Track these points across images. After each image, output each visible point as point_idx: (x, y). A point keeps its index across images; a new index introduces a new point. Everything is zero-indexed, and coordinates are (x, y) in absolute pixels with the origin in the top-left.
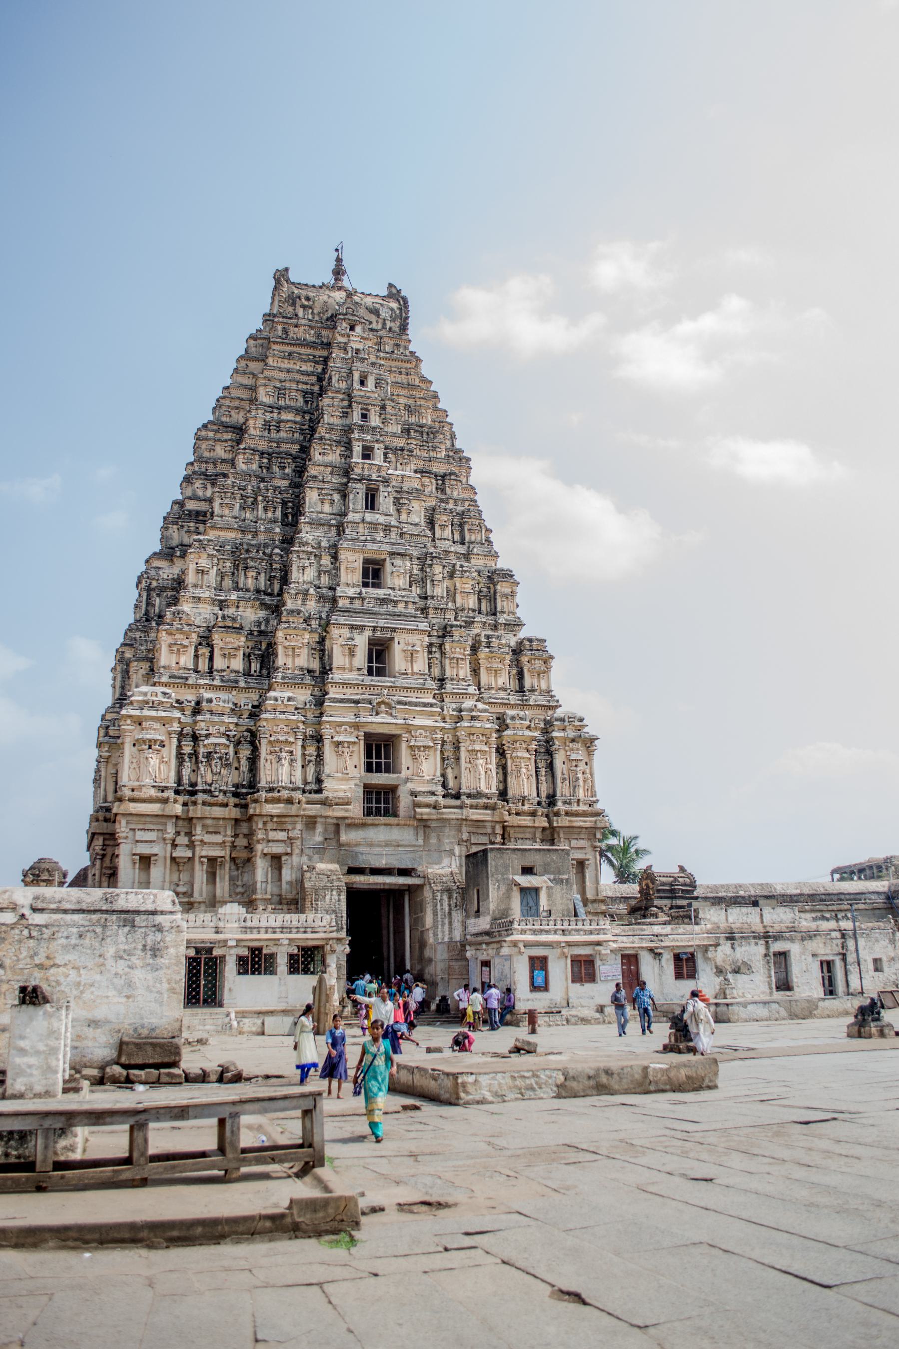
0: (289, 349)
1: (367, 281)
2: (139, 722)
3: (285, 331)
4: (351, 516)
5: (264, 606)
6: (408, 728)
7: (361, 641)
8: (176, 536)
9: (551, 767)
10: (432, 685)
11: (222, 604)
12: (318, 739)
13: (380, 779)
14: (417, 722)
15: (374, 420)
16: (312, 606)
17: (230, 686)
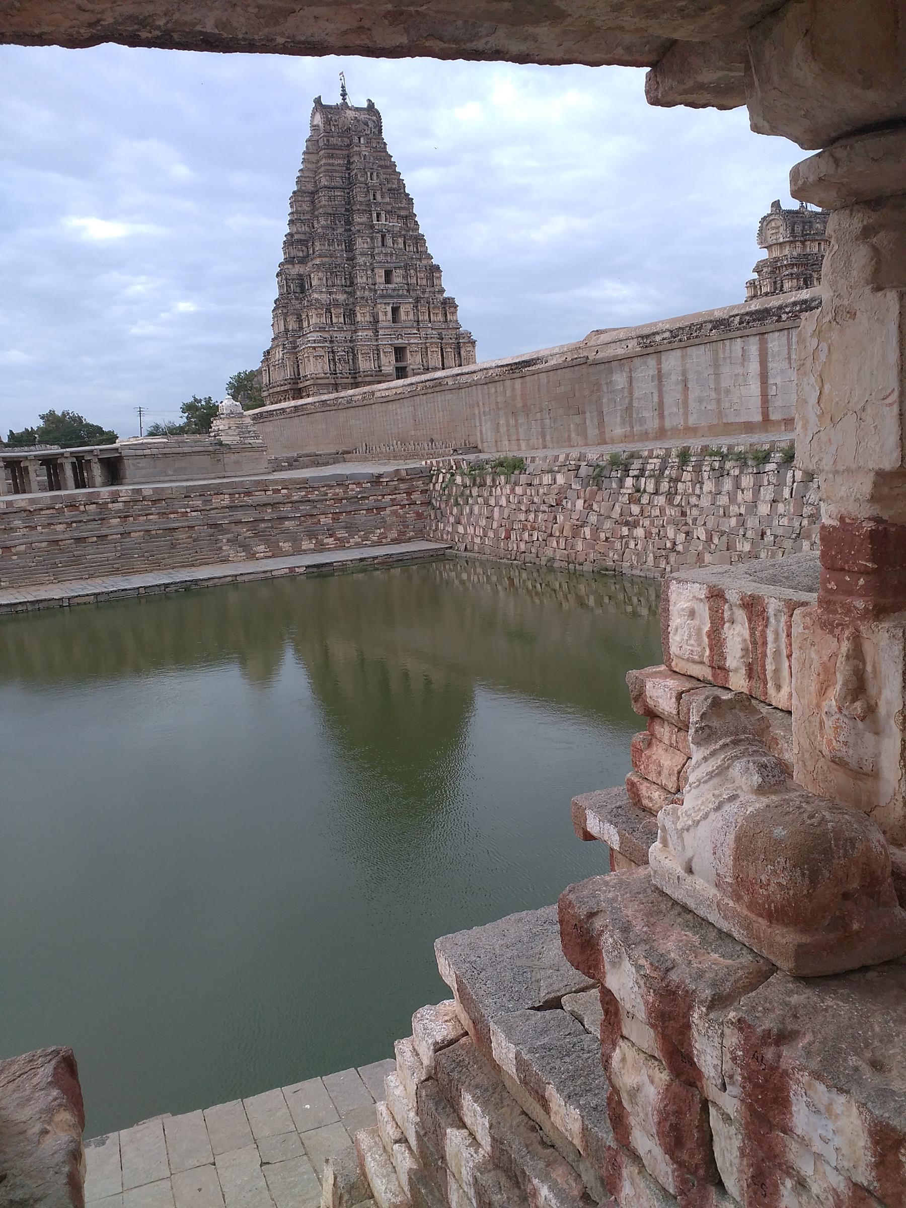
0: (331, 151)
1: (357, 100)
2: (314, 348)
3: (328, 141)
4: (376, 251)
5: (346, 292)
6: (409, 344)
7: (389, 309)
8: (294, 252)
9: (459, 353)
10: (415, 324)
11: (330, 293)
12: (378, 350)
13: (400, 364)
14: (412, 341)
15: (379, 197)
16: (367, 293)
17: (341, 330)
